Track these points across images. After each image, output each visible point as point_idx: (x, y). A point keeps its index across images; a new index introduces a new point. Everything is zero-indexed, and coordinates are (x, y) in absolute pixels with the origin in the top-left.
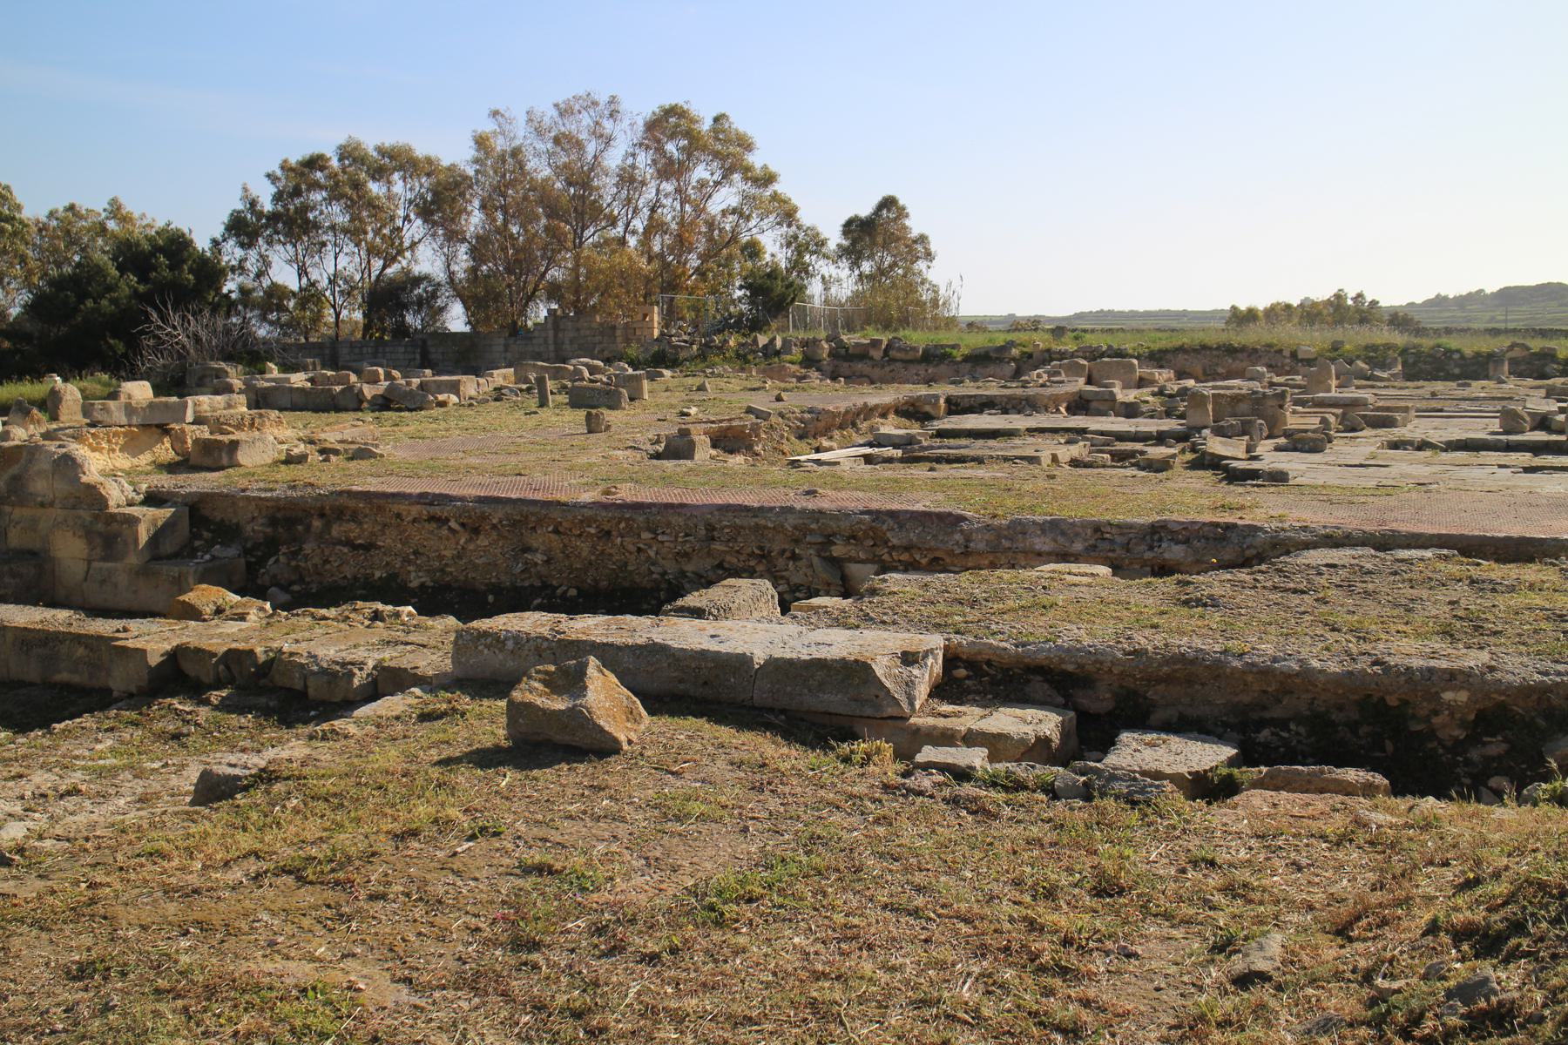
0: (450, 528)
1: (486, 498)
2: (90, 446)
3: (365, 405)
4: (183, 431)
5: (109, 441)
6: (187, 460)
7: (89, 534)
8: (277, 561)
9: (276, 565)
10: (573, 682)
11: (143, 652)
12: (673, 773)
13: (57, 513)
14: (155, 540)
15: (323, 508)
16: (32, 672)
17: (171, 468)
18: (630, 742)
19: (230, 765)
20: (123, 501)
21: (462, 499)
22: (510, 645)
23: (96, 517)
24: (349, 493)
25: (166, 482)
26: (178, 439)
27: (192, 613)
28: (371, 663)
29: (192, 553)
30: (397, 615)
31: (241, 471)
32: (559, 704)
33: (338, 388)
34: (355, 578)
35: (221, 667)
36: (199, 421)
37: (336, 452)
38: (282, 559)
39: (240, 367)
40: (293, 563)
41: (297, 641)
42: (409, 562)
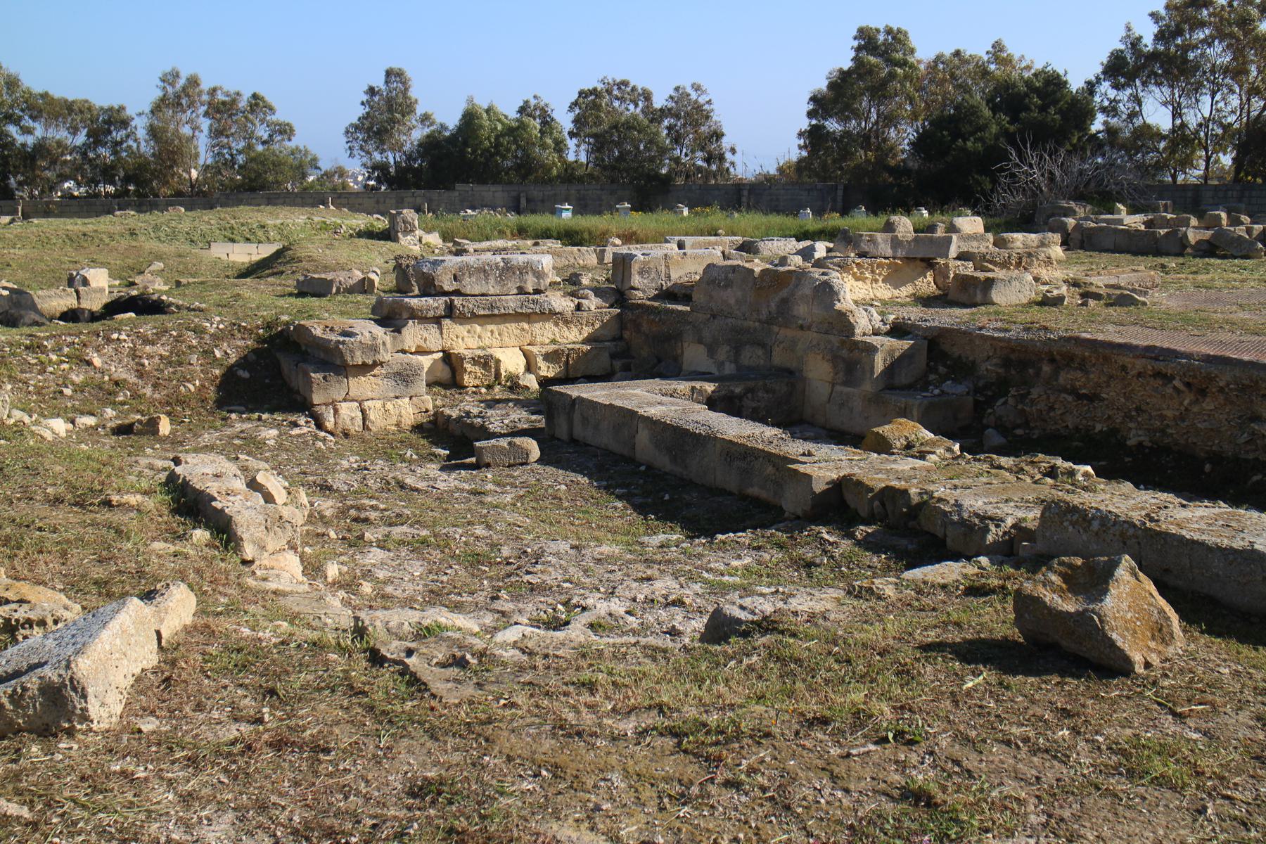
0: (1175, 388)
1: (1215, 357)
2: (854, 275)
3: (1189, 250)
4: (946, 265)
5: (873, 272)
6: (946, 295)
7: (835, 359)
8: (1005, 403)
9: (1004, 408)
10: (1093, 582)
11: (808, 477)
12: (1174, 714)
13: (812, 335)
14: (890, 370)
15: (1050, 352)
16: (732, 484)
17: (926, 301)
18: (1148, 665)
19: (742, 608)
20: (869, 329)
21: (1189, 356)
22: (1095, 525)
23: (843, 343)
24: (1078, 341)
25: (914, 314)
26: (941, 273)
27: (883, 446)
28: (1010, 521)
29: (925, 388)
30: (1071, 473)
31: (992, 309)
32: (1069, 605)
33: (1163, 232)
34: (1077, 429)
35: (876, 503)
36: (962, 257)
37: (1097, 297)
38: (1011, 401)
39: (1089, 207)
40: (1020, 407)
41: (956, 487)
42: (1131, 418)
